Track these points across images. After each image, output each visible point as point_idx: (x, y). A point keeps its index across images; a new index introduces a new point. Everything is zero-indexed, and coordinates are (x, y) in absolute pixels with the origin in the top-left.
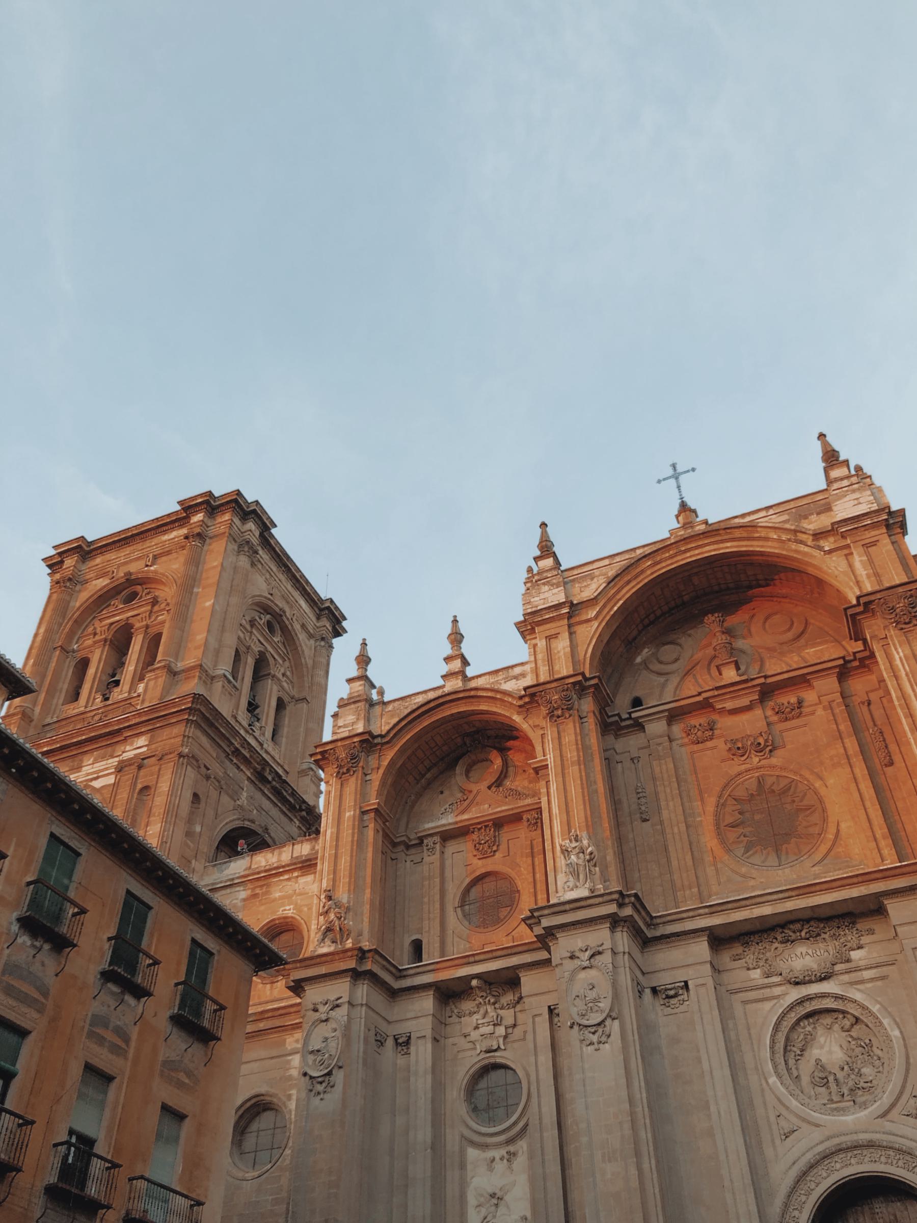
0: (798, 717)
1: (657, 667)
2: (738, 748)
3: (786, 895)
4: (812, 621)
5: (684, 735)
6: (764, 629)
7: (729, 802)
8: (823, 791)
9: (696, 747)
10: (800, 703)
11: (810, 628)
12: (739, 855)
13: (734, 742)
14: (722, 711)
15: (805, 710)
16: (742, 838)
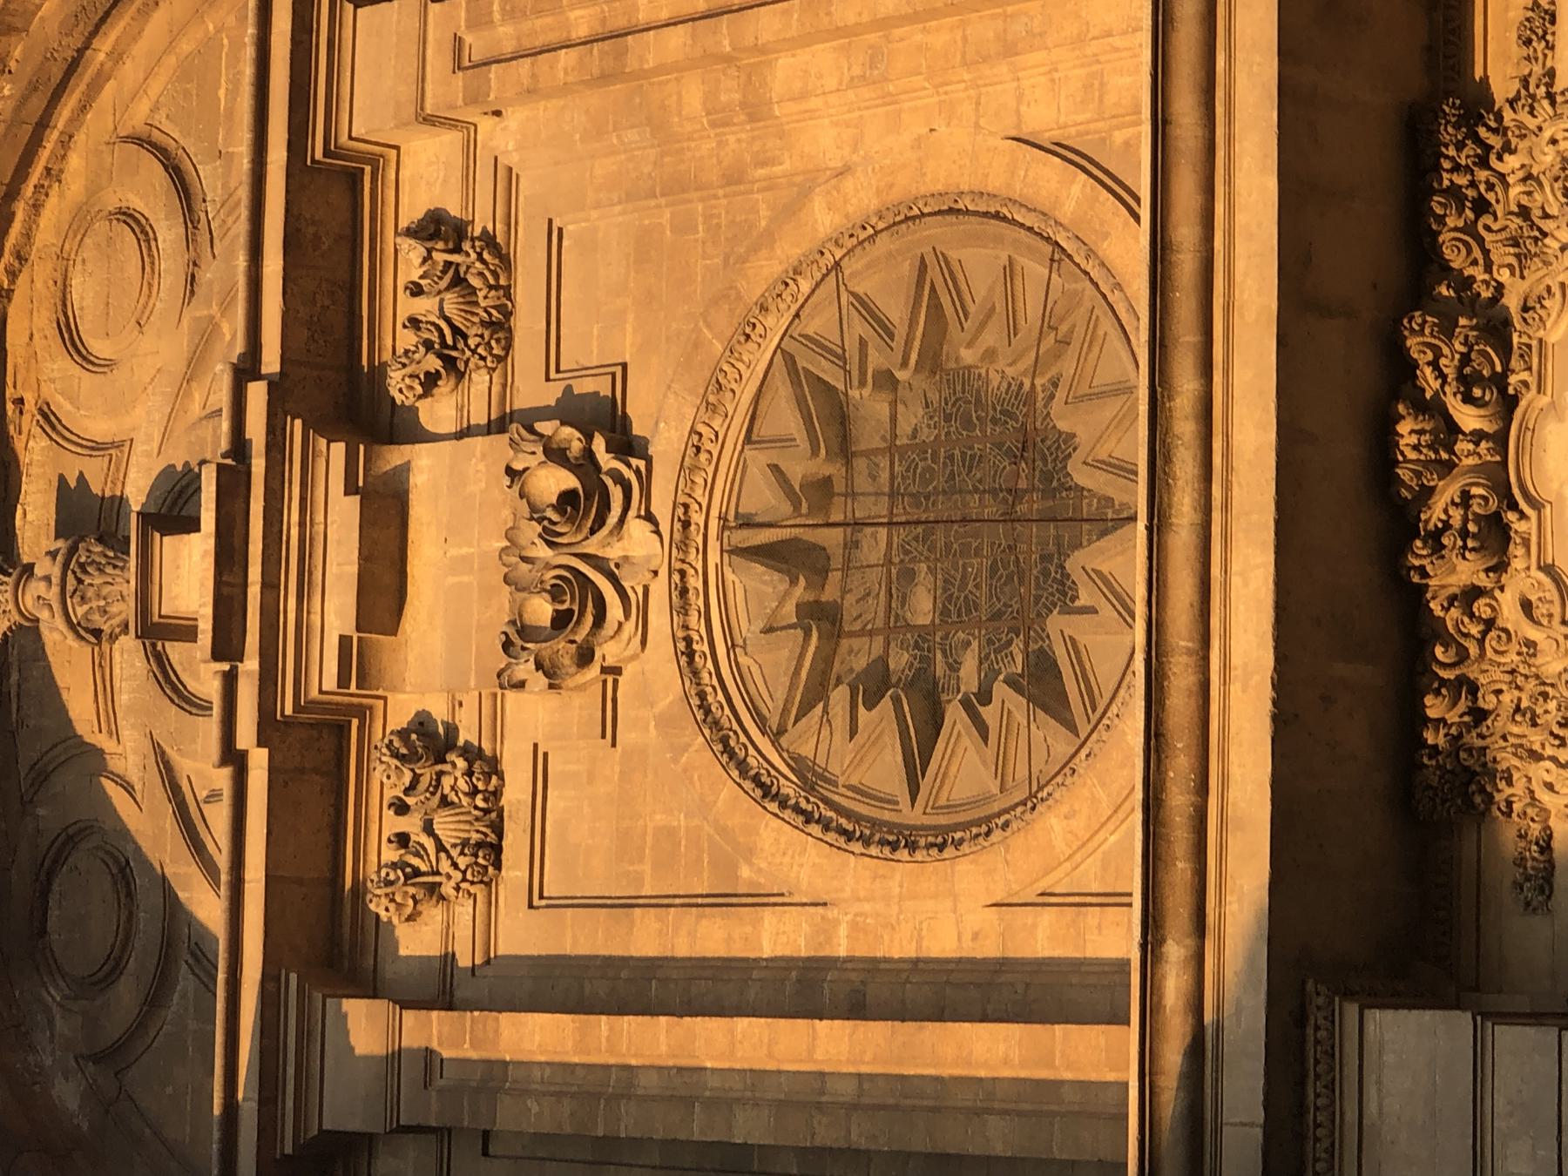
0: (506, 262)
1: (127, 994)
2: (561, 621)
3: (1184, 428)
4: (142, 110)
5: (434, 915)
6: (110, 364)
7: (807, 750)
8: (862, 197)
9: (514, 870)
10: (437, 229)
11: (173, 133)
12: (1062, 745)
13: (519, 635)
14: (357, 663)
15: (481, 222)
16: (989, 713)
